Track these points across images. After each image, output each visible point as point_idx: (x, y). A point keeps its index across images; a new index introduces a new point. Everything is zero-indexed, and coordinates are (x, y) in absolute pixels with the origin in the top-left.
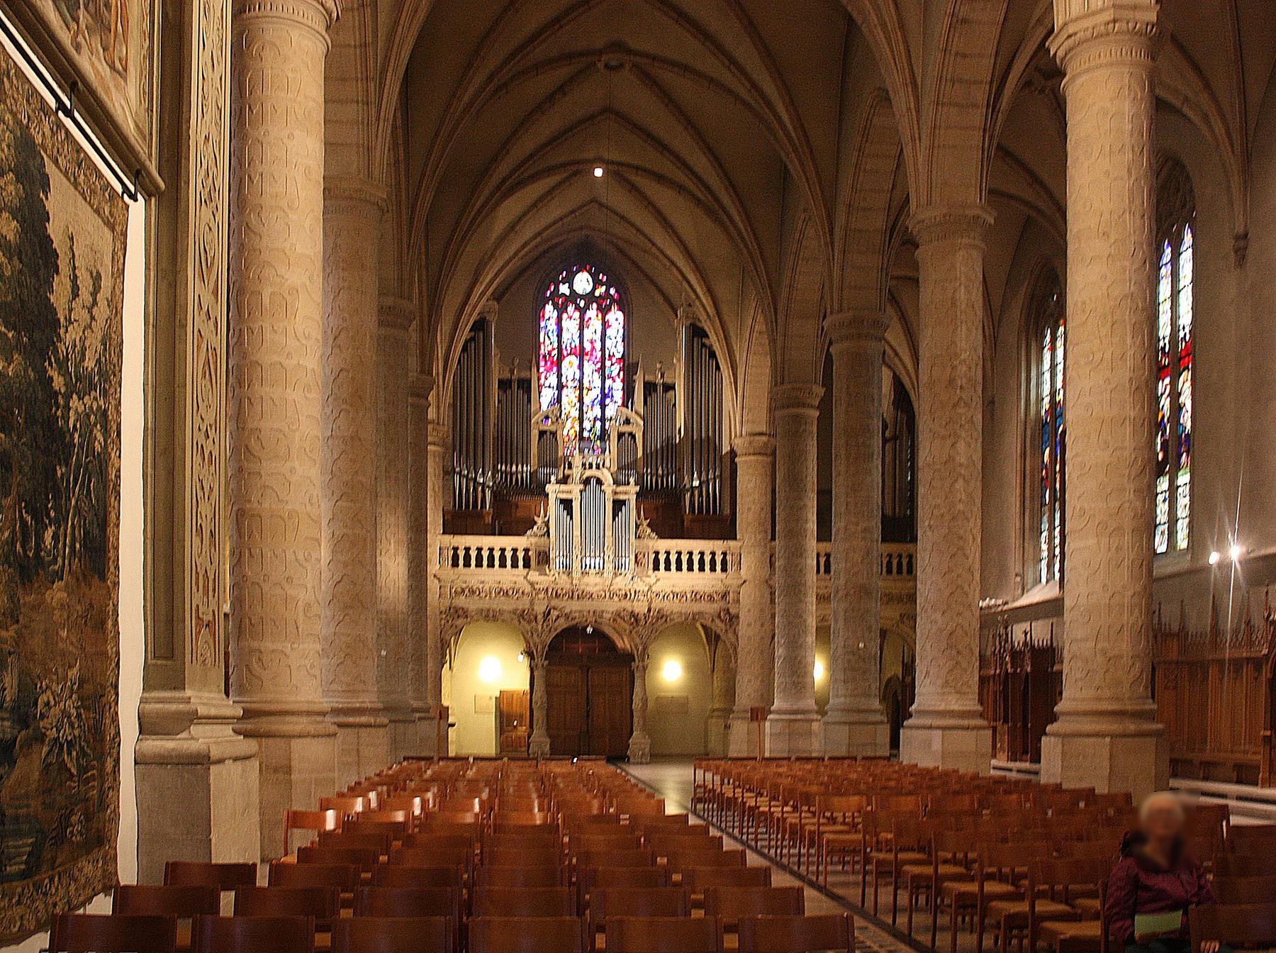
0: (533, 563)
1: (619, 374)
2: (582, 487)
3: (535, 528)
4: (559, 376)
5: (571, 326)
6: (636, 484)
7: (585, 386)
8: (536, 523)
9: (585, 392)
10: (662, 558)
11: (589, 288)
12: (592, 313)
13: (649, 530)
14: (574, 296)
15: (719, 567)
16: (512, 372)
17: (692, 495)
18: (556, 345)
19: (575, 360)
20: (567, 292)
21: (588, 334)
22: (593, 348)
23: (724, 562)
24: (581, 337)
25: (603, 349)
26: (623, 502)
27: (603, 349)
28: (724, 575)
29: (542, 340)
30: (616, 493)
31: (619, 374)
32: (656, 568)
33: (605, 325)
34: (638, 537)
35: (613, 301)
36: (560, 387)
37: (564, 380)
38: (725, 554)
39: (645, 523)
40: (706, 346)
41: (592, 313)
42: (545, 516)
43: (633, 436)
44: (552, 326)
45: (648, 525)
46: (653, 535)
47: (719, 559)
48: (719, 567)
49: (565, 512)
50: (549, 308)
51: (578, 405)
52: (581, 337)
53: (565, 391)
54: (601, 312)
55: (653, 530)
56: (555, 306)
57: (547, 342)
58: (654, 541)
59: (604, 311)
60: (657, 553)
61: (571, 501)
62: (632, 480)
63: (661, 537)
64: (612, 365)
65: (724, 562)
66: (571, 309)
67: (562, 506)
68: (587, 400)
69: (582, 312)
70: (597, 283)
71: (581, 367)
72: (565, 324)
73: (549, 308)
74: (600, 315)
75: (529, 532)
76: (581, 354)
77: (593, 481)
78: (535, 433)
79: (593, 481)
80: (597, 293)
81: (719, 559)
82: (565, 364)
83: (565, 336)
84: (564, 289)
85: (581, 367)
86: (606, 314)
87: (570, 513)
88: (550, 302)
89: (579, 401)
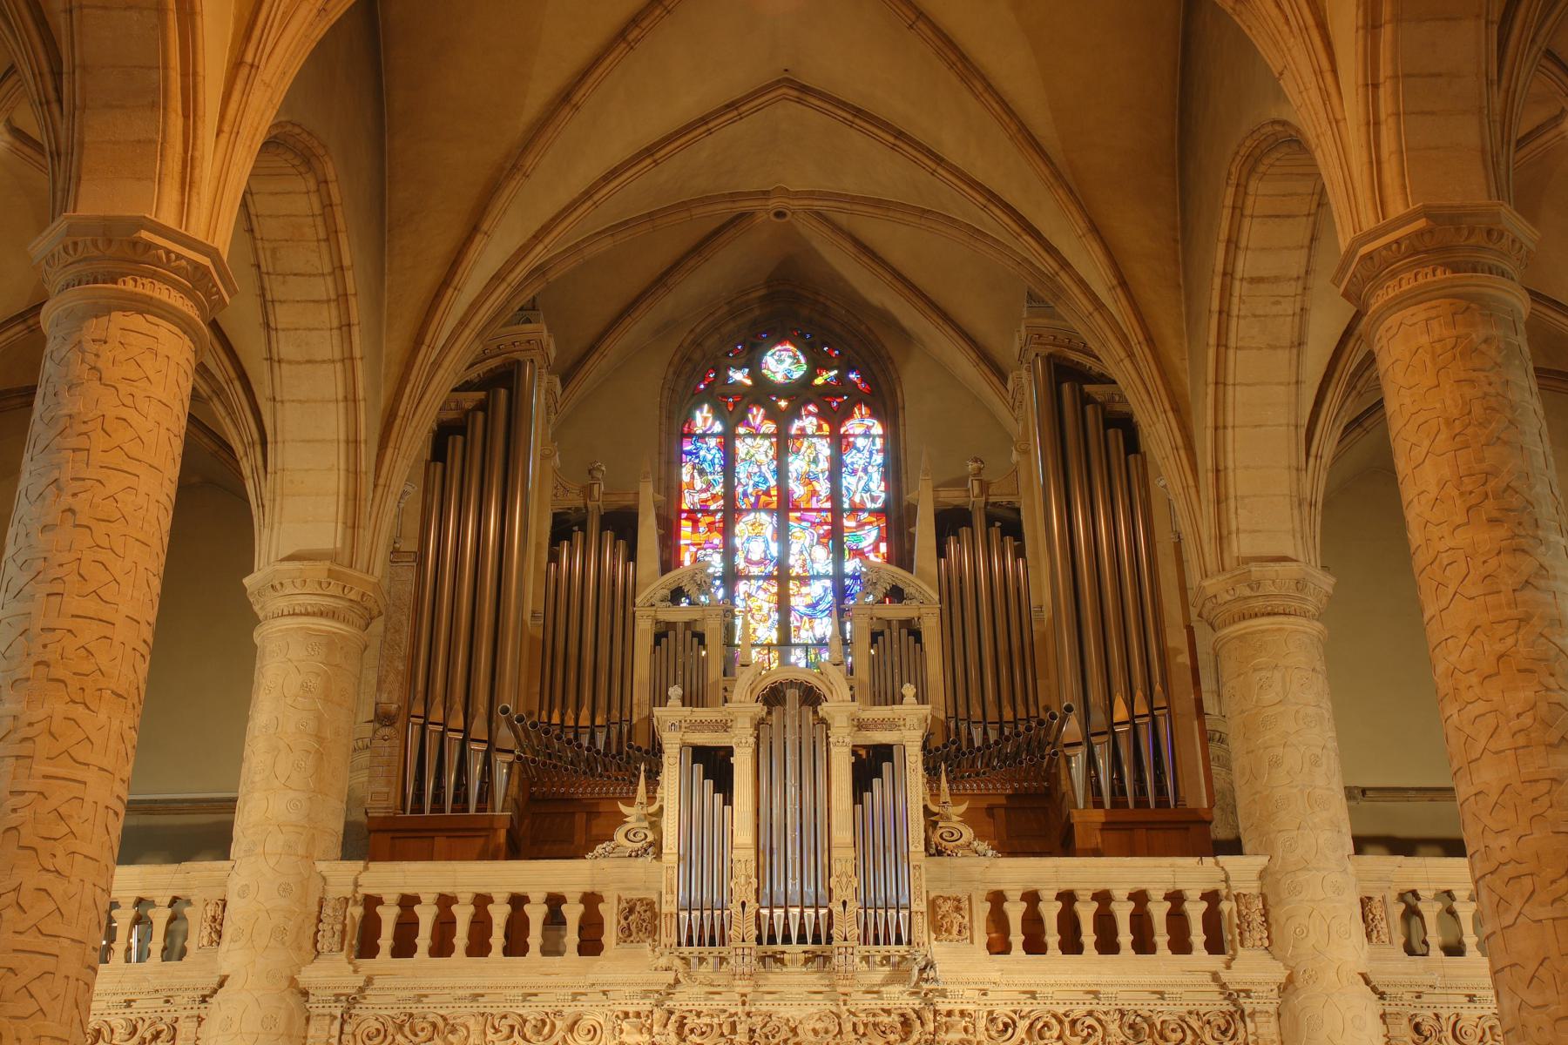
0: (610, 936)
1: (876, 549)
2: (760, 709)
3: (619, 835)
4: (729, 552)
5: (755, 452)
6: (922, 698)
7: (793, 572)
8: (620, 819)
9: (793, 586)
10: (1015, 912)
11: (797, 374)
12: (809, 423)
13: (968, 834)
14: (763, 392)
15: (1198, 937)
16: (587, 491)
17: (1091, 761)
18: (719, 489)
19: (767, 522)
20: (749, 382)
21: (797, 465)
22: (814, 493)
23: (1212, 922)
24: (781, 472)
25: (835, 495)
26: (884, 753)
27: (835, 495)
28: (1217, 962)
29: (686, 478)
30: (861, 726)
31: (876, 549)
32: (999, 946)
33: (840, 443)
34: (935, 851)
35: (857, 399)
36: (731, 577)
37: (740, 561)
38: (1212, 898)
39: (956, 811)
40: (1094, 402)
41: (809, 423)
42: (651, 799)
43: (913, 631)
44: (710, 451)
45: (967, 818)
46: (982, 846)
47: (1195, 911)
48: (1198, 937)
49: (709, 784)
50: (703, 419)
51: (775, 616)
52: (781, 472)
53: (742, 587)
54: (828, 422)
55: (979, 836)
56: (718, 413)
57: (699, 484)
58: (985, 862)
59: (834, 417)
60: (997, 899)
61: (729, 751)
62: (909, 690)
63: (1012, 846)
64: (861, 525)
65: (1212, 922)
66: (757, 415)
67: (699, 769)
68: (798, 603)
69: (783, 420)
70: (815, 367)
71: (782, 534)
72: (741, 447)
73: (703, 419)
74: (826, 427)
75: (599, 849)
76: (785, 506)
77: (792, 695)
78: (644, 629)
79: (792, 695)
80: (819, 381)
81: (1195, 911)
82: (742, 528)
83: (742, 470)
84: (739, 376)
85: (782, 534)
86: (841, 423)
87: (724, 784)
88: (706, 407)
89: (779, 610)
